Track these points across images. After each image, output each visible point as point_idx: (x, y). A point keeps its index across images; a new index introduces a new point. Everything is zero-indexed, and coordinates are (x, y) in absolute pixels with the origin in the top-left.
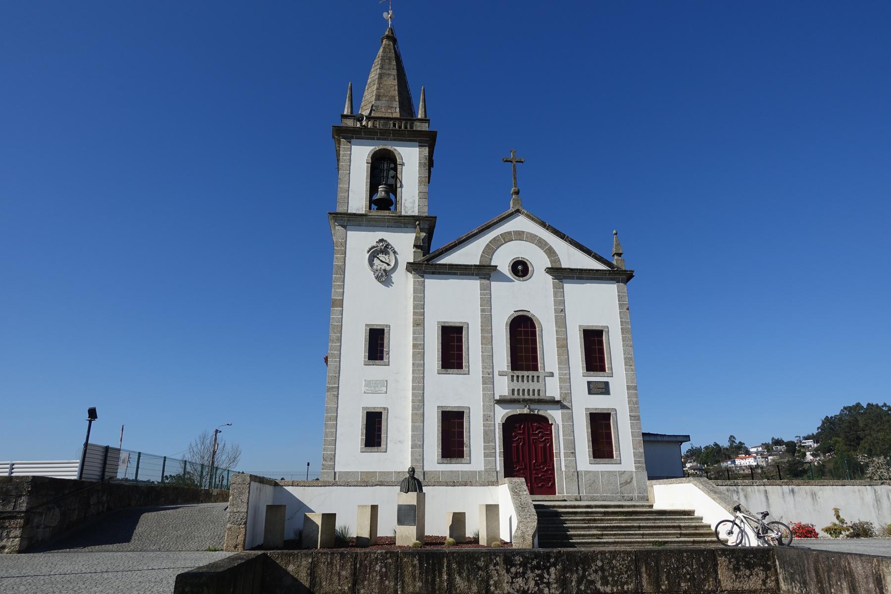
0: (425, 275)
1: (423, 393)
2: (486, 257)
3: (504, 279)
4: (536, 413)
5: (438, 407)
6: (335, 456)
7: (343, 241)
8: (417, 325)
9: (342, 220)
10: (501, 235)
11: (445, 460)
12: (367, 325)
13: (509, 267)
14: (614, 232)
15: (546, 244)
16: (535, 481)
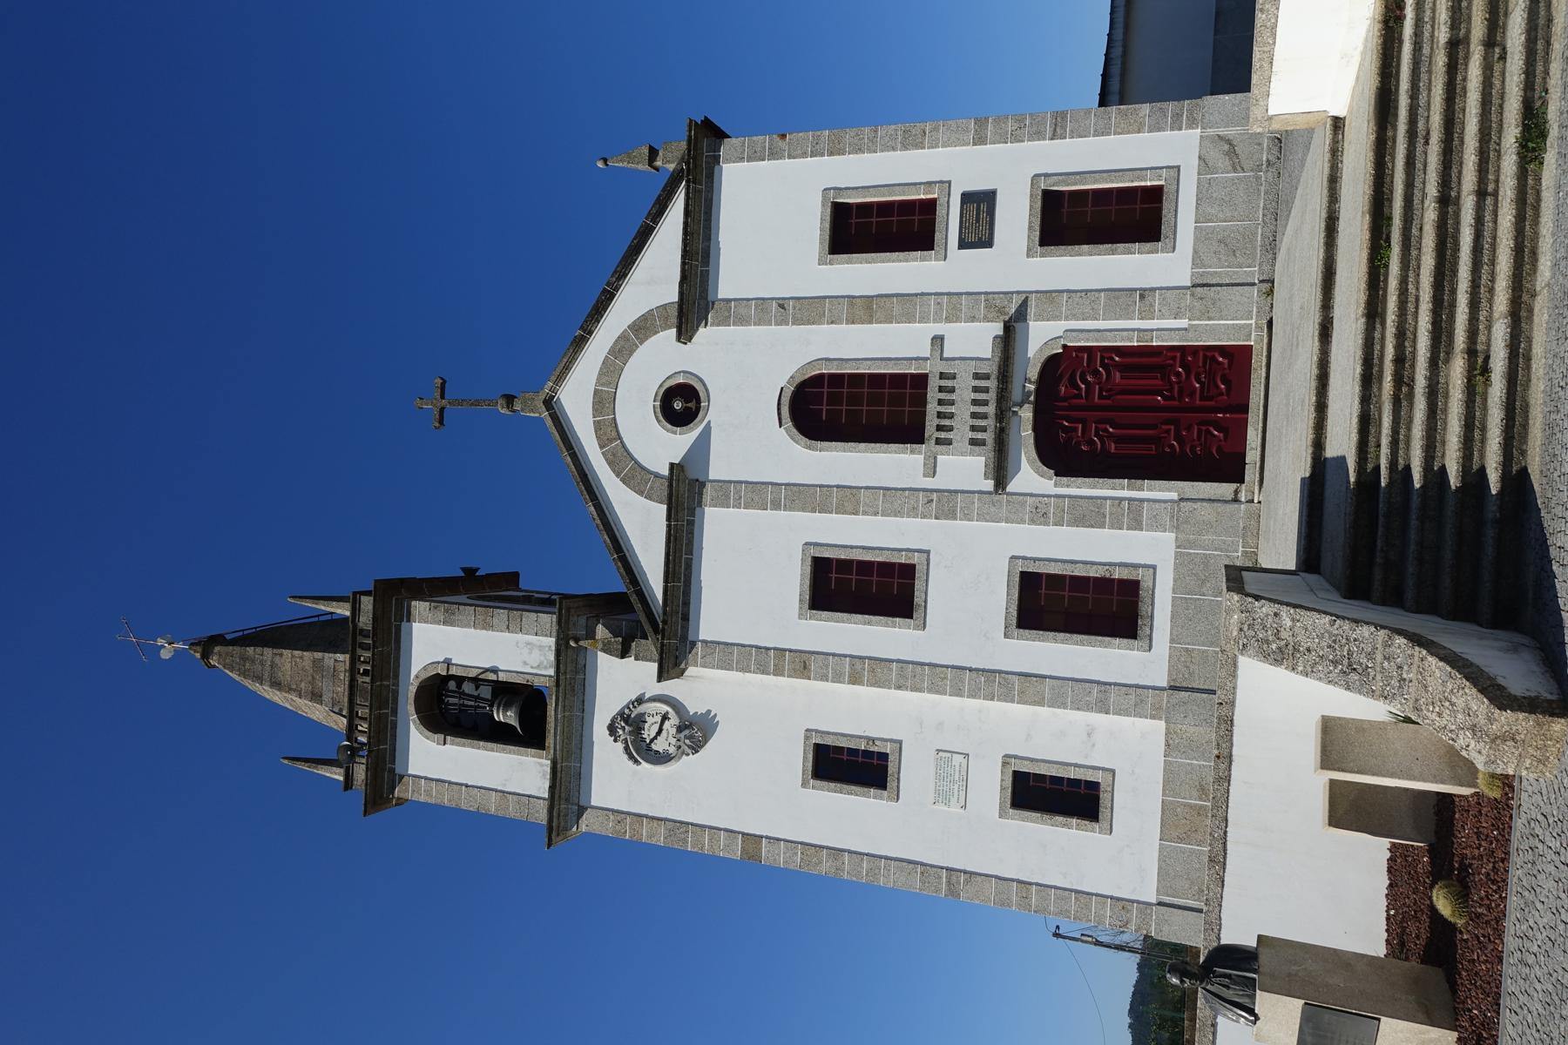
0: (690, 638)
1: (971, 670)
2: (651, 488)
3: (703, 444)
4: (1032, 387)
5: (1006, 636)
6: (1118, 899)
7: (612, 817)
8: (805, 667)
9: (566, 815)
10: (601, 447)
11: (1143, 631)
12: (804, 785)
13: (675, 433)
14: (600, 164)
15: (623, 337)
16: (1211, 399)
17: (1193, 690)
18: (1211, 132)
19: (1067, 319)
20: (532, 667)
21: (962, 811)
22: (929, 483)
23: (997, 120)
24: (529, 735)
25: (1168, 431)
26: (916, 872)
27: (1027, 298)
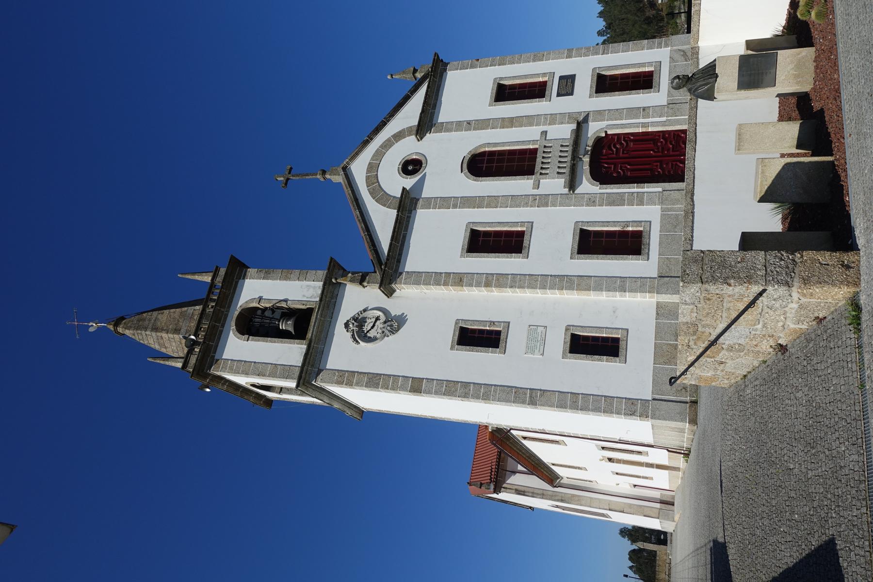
0: (400, 271)
1: (551, 276)
2: (391, 202)
3: (420, 184)
4: (590, 148)
5: (571, 258)
6: (630, 399)
7: (337, 374)
8: (461, 281)
9: (310, 374)
10: (367, 187)
11: (644, 251)
12: (452, 348)
13: (407, 178)
14: (389, 77)
15: (389, 140)
16: (678, 151)
17: (671, 277)
18: (675, 48)
19: (607, 120)
20: (307, 298)
21: (541, 356)
22: (535, 192)
23: (578, 49)
24: (299, 334)
25: (657, 166)
26: (512, 392)
27: (588, 113)
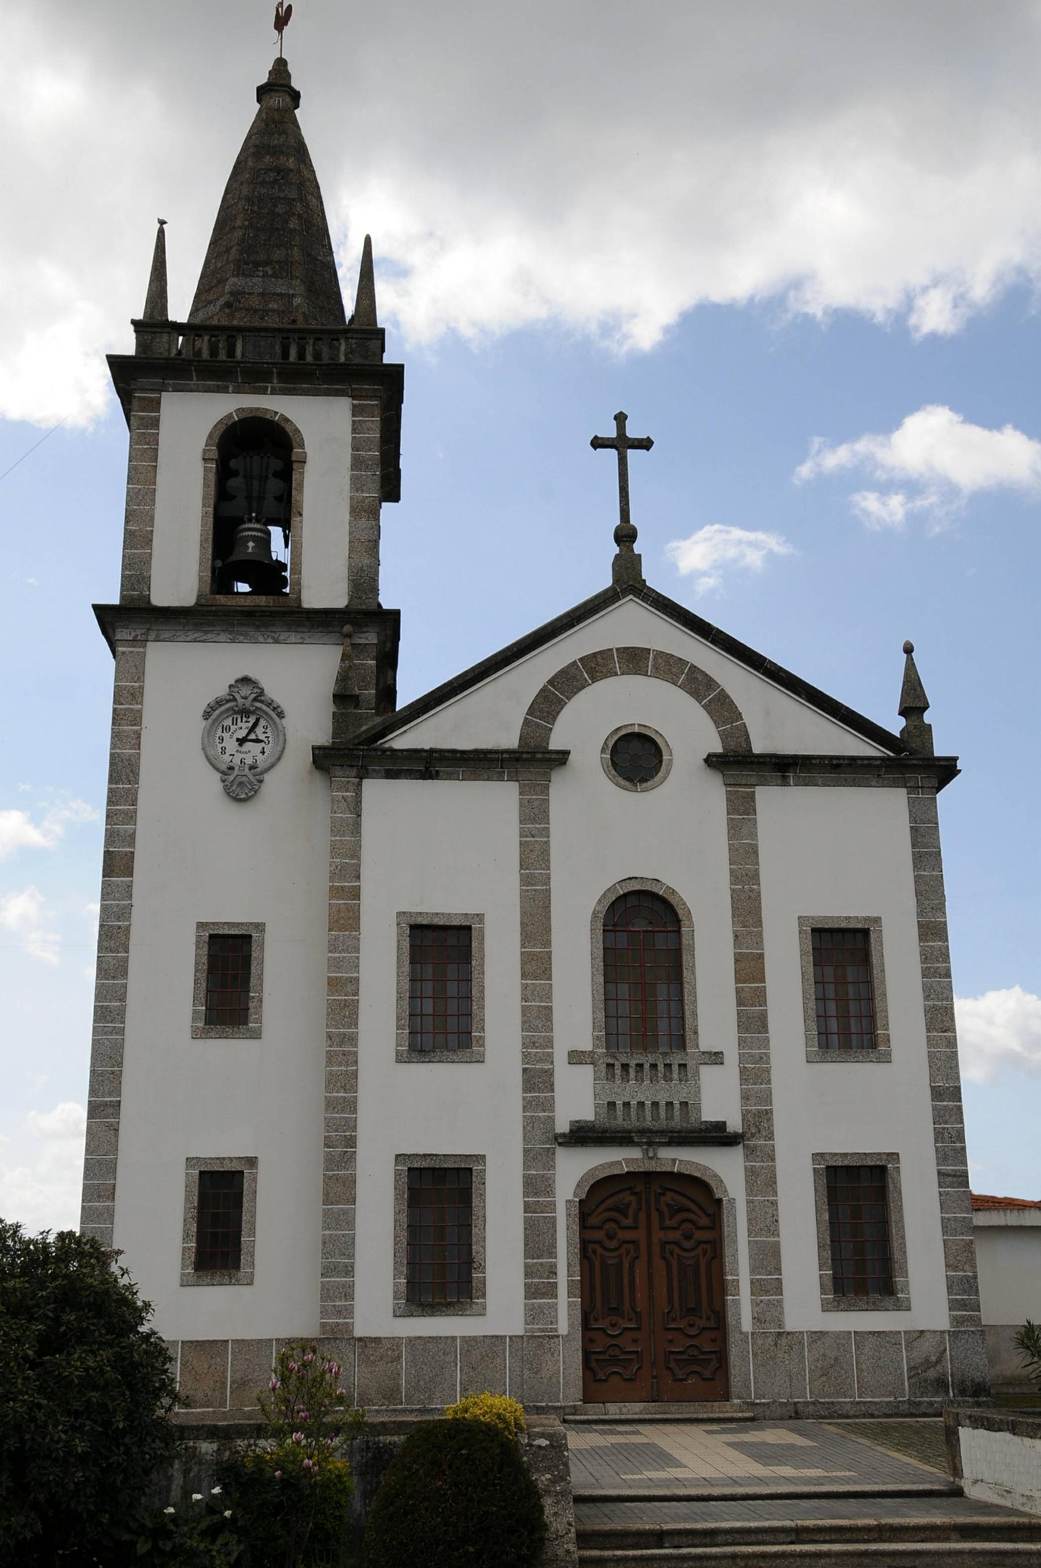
12: (201, 926)
13: (603, 751)
15: (710, 683)
